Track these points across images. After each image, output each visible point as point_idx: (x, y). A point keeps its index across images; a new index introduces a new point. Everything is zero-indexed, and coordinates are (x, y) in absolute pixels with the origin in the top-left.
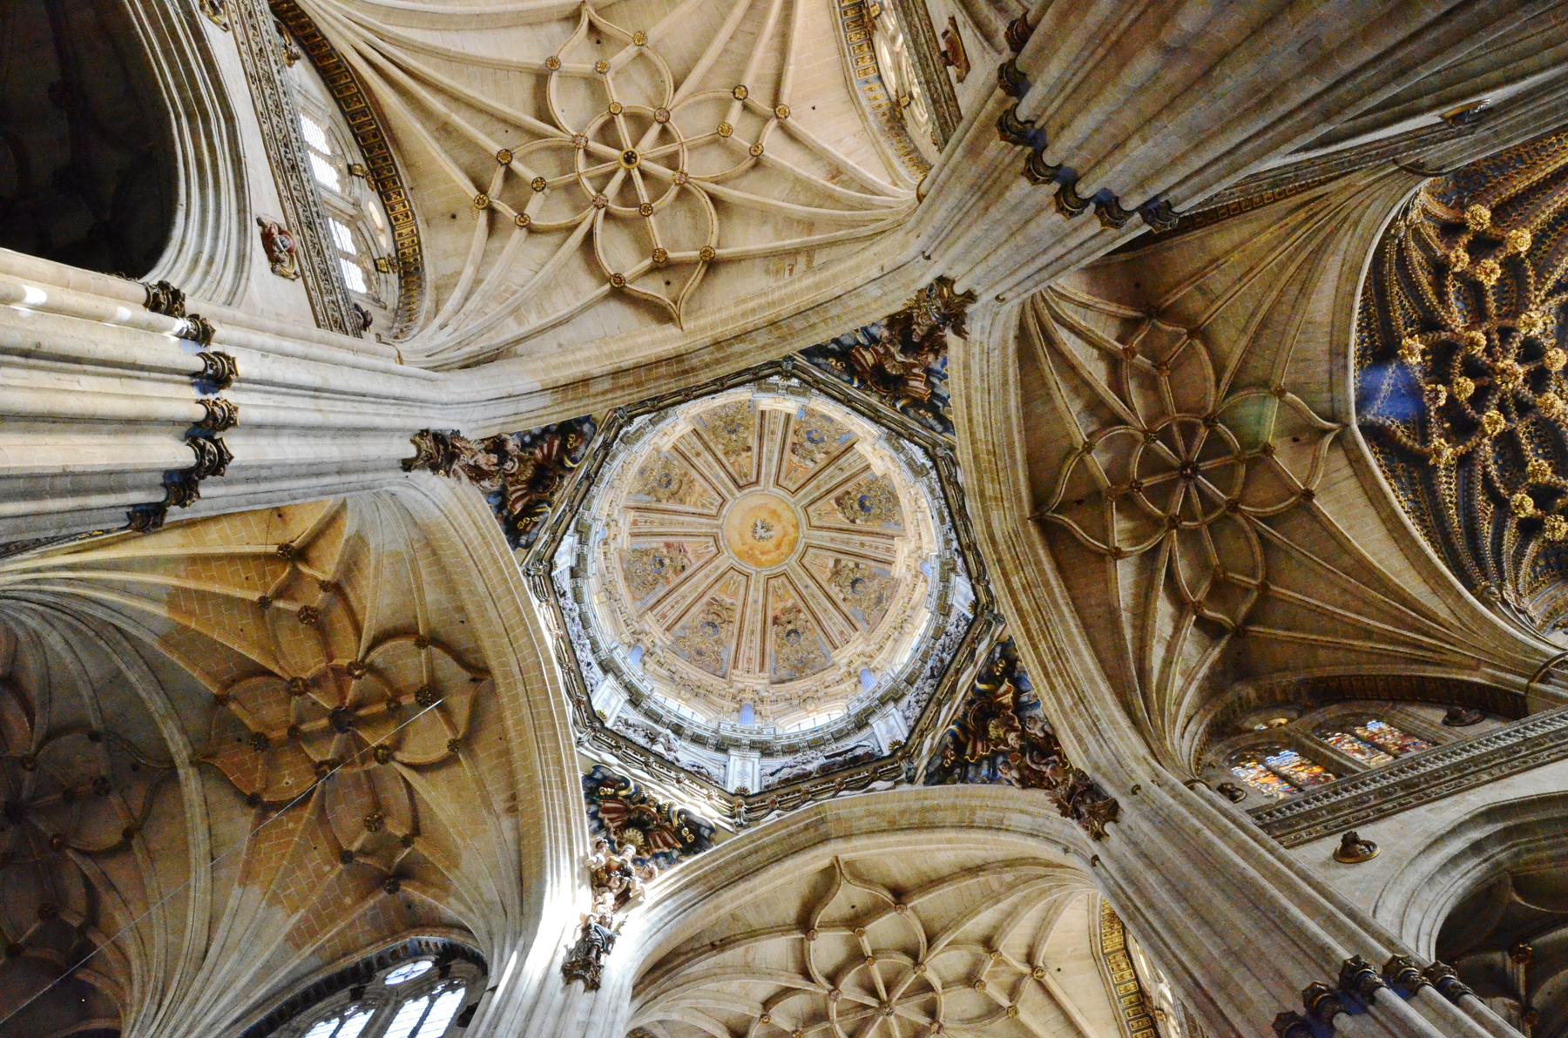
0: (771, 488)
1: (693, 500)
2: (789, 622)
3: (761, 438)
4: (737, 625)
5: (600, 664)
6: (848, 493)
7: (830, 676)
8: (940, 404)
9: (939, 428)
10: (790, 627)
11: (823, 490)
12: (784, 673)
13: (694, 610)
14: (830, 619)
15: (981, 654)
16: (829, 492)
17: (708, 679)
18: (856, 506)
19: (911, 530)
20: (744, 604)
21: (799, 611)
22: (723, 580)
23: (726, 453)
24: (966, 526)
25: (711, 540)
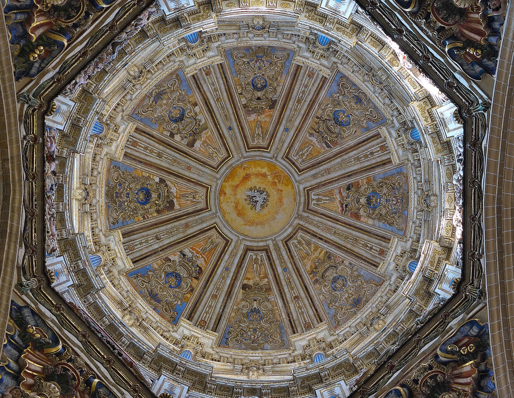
0: (235, 239)
1: (317, 254)
2: (259, 99)
3: (229, 294)
4: (313, 113)
5: (451, 152)
6: (158, 212)
7: (231, 42)
8: (16, 338)
9: (26, 312)
10: (259, 94)
11: (183, 222)
12: (279, 54)
13: (352, 143)
14: (216, 90)
15: (54, 68)
16: (177, 218)
17: (357, 79)
18: (154, 196)
19: (103, 166)
20: (299, 131)
21: (245, 106)
22: (313, 161)
23: (269, 290)
24: (31, 199)
25: (312, 206)
